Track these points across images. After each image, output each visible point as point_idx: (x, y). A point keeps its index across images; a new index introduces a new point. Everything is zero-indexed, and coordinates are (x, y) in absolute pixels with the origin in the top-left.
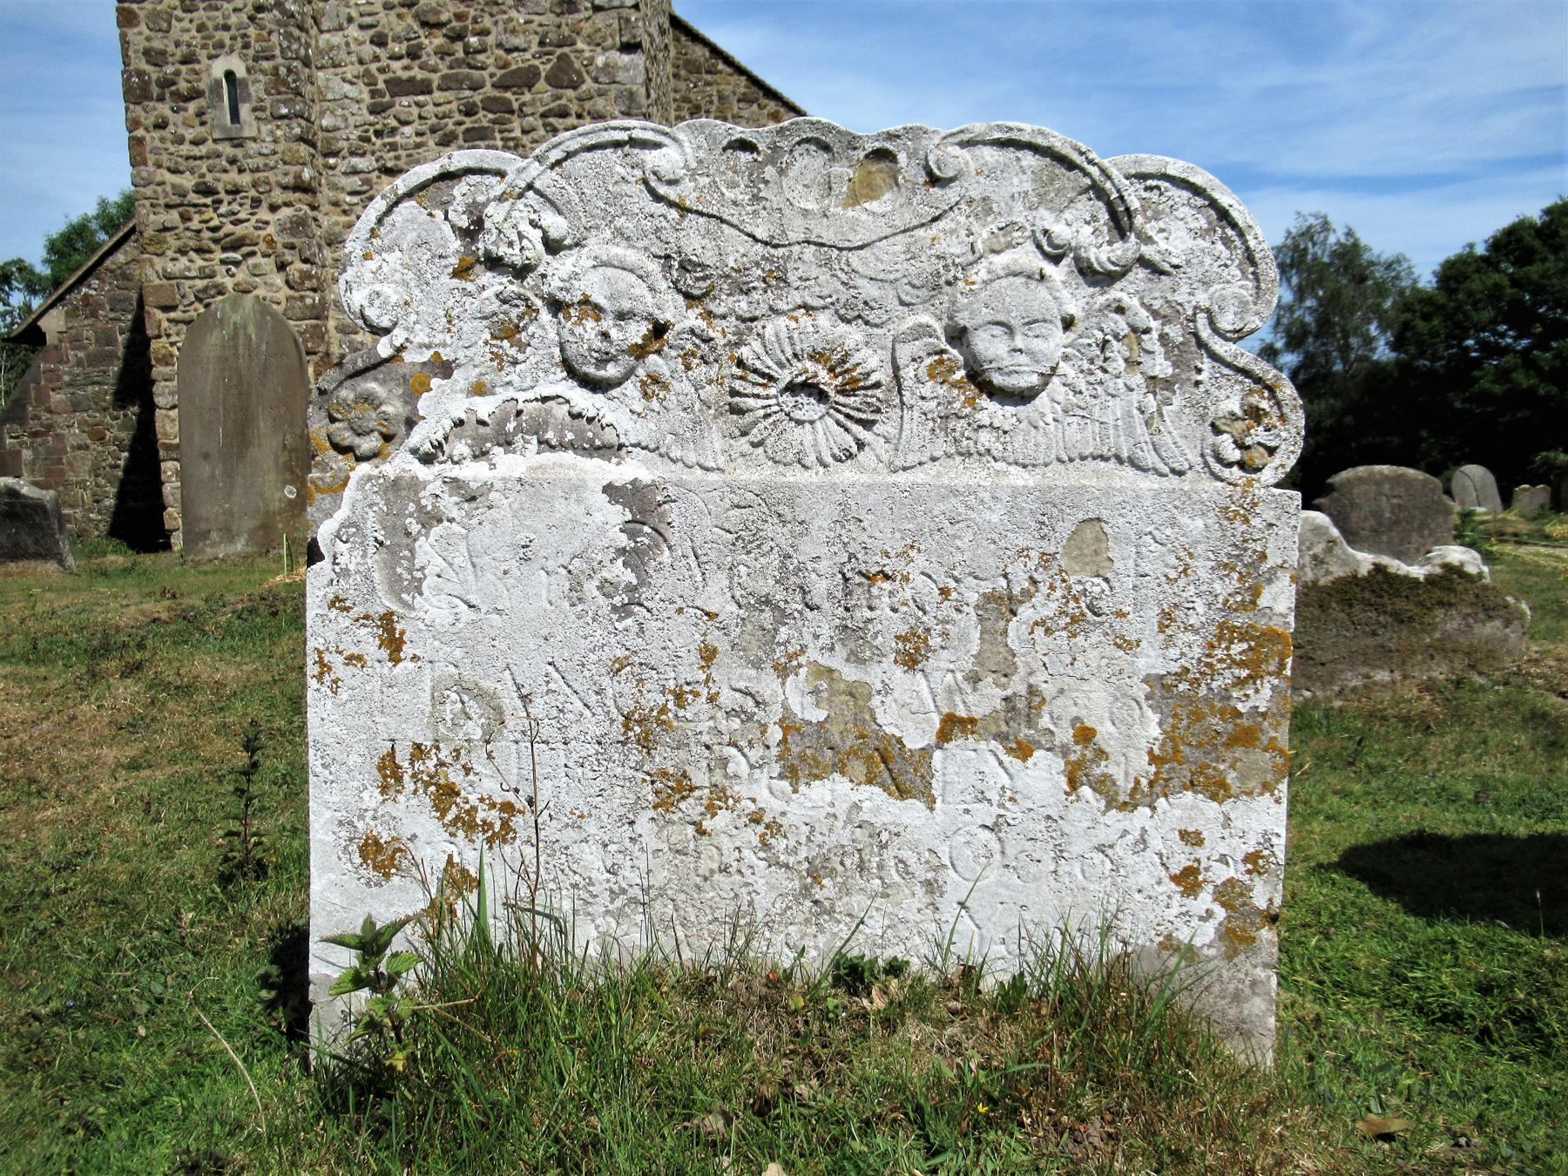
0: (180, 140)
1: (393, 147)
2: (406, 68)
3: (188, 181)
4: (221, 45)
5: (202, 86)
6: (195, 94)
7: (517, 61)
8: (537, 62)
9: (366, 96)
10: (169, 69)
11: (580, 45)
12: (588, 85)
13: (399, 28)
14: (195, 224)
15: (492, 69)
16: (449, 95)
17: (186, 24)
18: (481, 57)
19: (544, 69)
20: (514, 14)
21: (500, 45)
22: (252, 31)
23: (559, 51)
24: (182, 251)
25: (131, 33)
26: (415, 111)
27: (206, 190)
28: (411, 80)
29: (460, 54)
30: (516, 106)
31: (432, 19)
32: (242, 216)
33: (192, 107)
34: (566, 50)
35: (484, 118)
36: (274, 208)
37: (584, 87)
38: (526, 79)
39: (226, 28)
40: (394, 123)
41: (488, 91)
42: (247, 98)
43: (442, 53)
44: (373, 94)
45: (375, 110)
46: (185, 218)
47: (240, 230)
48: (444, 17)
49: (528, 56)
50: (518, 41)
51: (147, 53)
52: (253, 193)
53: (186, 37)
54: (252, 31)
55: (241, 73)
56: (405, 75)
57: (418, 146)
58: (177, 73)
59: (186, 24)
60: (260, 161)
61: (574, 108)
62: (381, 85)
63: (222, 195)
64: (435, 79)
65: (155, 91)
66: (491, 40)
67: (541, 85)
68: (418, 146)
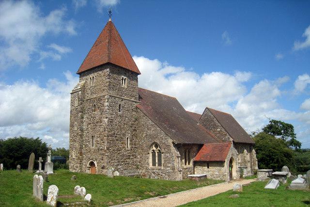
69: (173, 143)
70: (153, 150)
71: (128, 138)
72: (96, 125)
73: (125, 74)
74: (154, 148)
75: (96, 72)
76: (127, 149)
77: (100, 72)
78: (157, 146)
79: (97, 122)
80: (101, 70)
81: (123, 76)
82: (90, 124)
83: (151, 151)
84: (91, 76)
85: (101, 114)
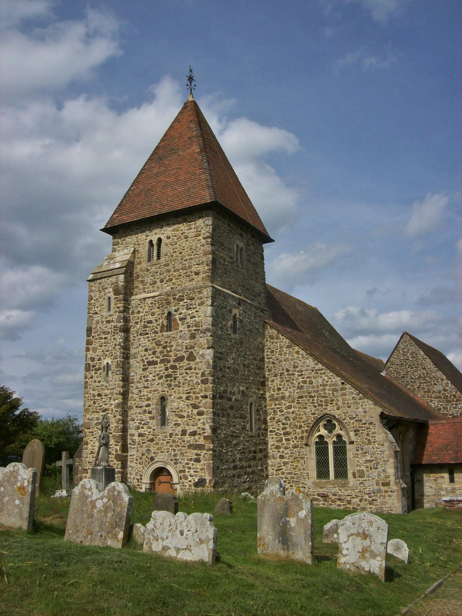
0: (95, 382)
1: (147, 381)
2: (152, 358)
3: (96, 393)
4: (106, 355)
5: (102, 367)
6: (99, 369)
7: (179, 354)
8: (184, 354)
9: (142, 366)
10: (95, 362)
11: (196, 348)
12: (198, 360)
13: (151, 346)
14: (96, 405)
15: (173, 357)
16: (162, 365)
17: (100, 350)
18: (170, 353)
19: (186, 356)
20: (179, 341)
21: (175, 350)
22: (114, 352)
23: (190, 350)
24: (93, 412)
25: (88, 353)
26: (153, 369)
27: (99, 395)
28: (153, 361)
29: (166, 353)
30: (178, 367)
31: (159, 344)
32: (107, 403)
33: (99, 372)
34: (192, 350)
35: (170, 371)
36: (114, 400)
37: (196, 361)
38: (181, 359)
39: (108, 351)
40: (148, 374)
41: (172, 363)
42: (110, 370)
43: (161, 352)
44: (144, 365)
45: (144, 370)
46: (94, 403)
47: (105, 407)
48: (162, 343)
49: (182, 352)
50: (180, 348)
51: (91, 358)
52: (110, 396)
53: (99, 354)
54: (114, 352)
55: (110, 363)
56: (151, 360)
57: (153, 380)
58: (96, 363)
59: (100, 350)
60: (112, 387)
61: (193, 367)
62: (146, 363)
63: (103, 397)
64: (159, 360)
65: (92, 368)
66: (173, 348)
67: (185, 360)
68: (153, 380)
69: (382, 416)
70: (321, 437)
71: (251, 404)
72: (174, 367)
73: (241, 235)
74: (323, 432)
75: (169, 225)
76: (250, 433)
77: (183, 227)
78: (330, 427)
79: (181, 359)
80: (185, 221)
81: (238, 242)
82: (151, 363)
83: (314, 439)
84: (154, 235)
85: (193, 337)
